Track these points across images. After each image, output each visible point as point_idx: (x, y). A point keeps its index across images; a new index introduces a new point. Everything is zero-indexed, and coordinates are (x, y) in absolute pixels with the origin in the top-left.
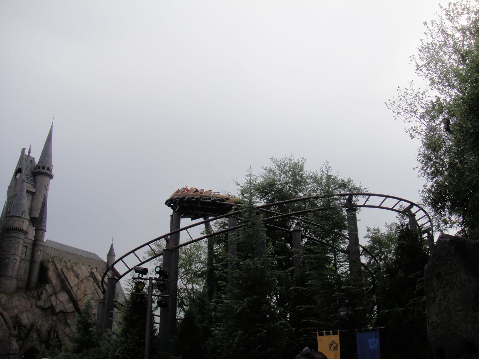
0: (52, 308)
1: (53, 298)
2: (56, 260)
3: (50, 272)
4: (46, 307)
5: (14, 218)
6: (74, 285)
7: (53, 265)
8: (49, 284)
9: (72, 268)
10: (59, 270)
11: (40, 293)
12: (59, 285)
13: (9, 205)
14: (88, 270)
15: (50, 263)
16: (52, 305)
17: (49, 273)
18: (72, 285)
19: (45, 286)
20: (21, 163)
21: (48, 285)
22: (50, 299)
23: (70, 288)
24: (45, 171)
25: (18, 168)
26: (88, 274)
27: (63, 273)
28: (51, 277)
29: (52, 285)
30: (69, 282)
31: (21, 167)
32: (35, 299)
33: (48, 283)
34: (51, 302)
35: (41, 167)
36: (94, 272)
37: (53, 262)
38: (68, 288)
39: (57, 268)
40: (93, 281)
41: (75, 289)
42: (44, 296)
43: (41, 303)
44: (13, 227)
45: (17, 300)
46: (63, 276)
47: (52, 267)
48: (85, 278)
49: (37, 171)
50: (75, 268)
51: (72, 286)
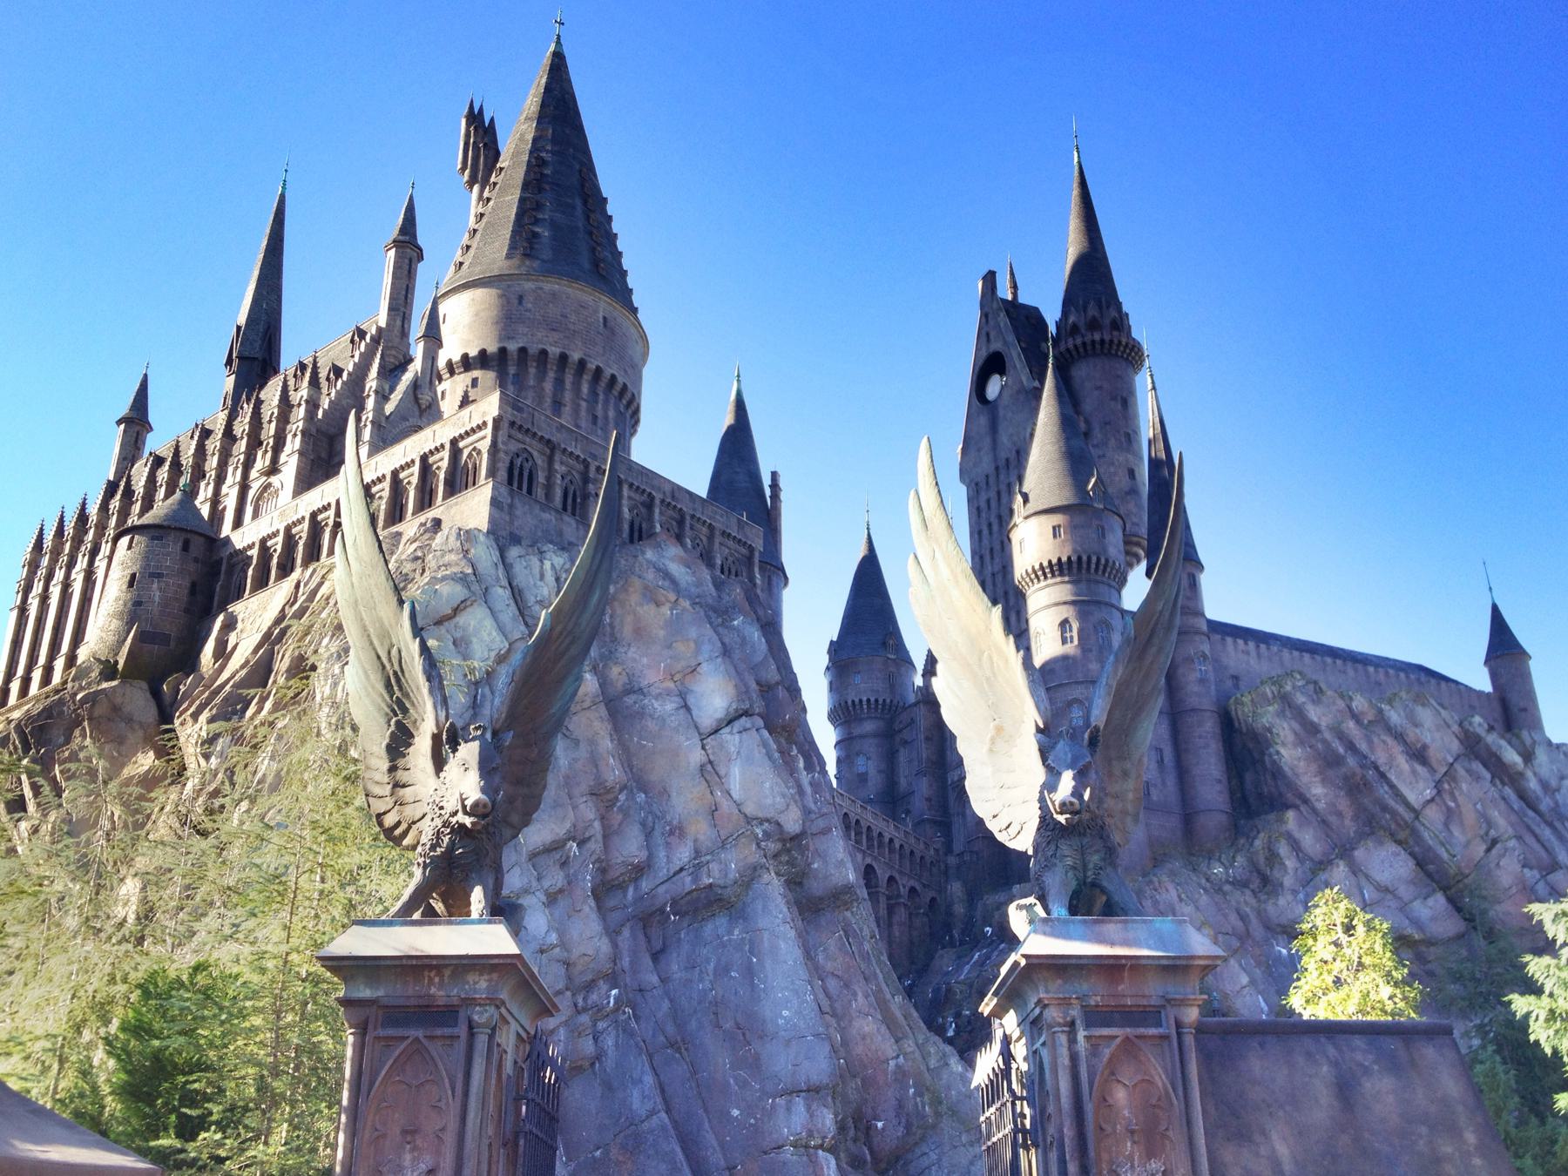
2: (1294, 687)
3: (1283, 751)
6: (1422, 800)
7: (1288, 713)
8: (1296, 807)
9: (1381, 720)
10: (1328, 735)
11: (1262, 860)
12: (1344, 804)
14: (1449, 726)
15: (1270, 708)
17: (1278, 753)
19: (1281, 821)
26: (1455, 746)
27: (1351, 747)
28: (1297, 775)
29: (1314, 811)
30: (1392, 786)
32: (1248, 892)
33: (1287, 807)
36: (1482, 732)
38: (1394, 813)
39: (1312, 729)
40: (1488, 776)
41: (1433, 815)
45: (1181, 900)
47: (1285, 725)
48: (1456, 760)
50: (1395, 717)
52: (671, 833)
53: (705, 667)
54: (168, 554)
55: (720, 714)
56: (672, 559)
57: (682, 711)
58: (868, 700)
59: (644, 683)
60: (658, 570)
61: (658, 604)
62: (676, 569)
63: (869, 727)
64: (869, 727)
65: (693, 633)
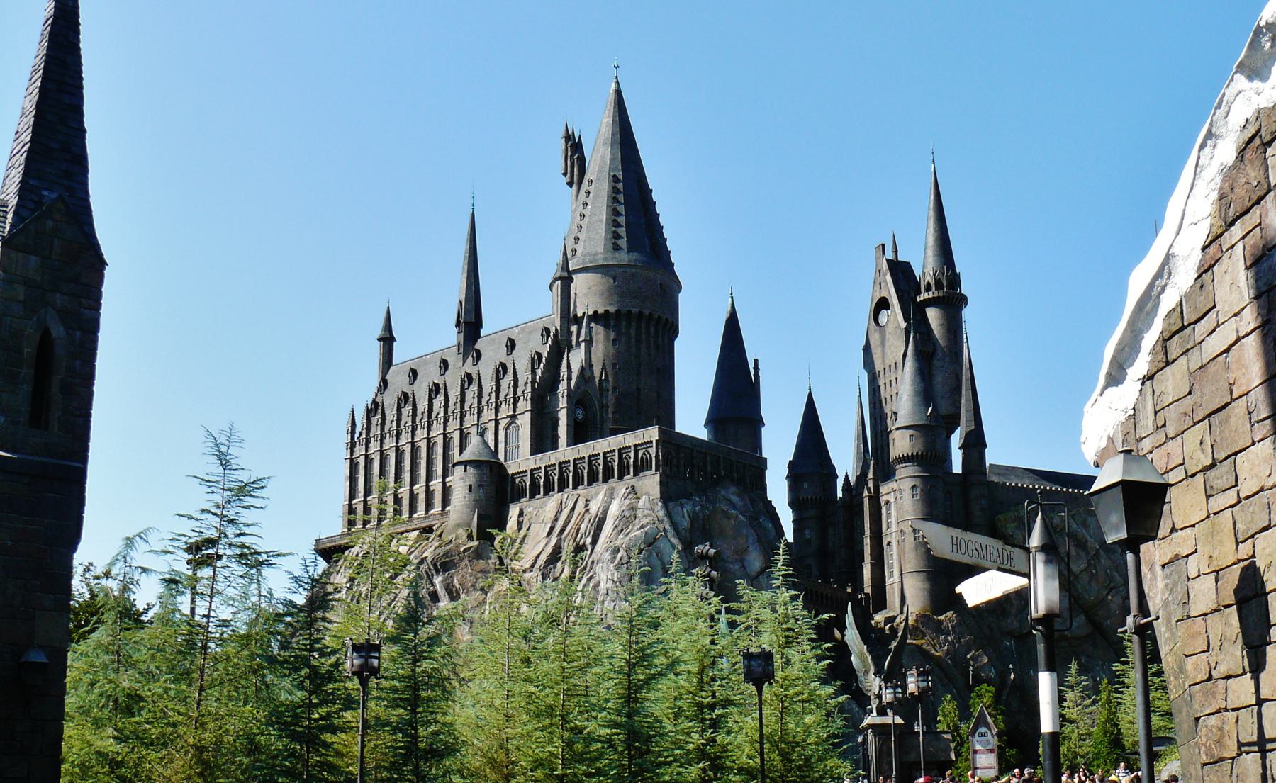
4: (1024, 632)
31: (884, 294)
53: (751, 548)
56: (733, 494)
58: (811, 498)
60: (727, 500)
62: (735, 498)
63: (812, 513)
64: (812, 513)
65: (745, 531)
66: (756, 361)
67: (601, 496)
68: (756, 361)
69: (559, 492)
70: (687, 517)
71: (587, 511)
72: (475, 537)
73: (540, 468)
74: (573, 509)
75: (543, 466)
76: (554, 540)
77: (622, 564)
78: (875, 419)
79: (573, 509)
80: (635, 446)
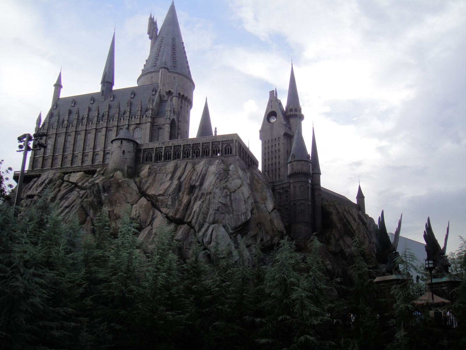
0: (342, 252)
1: (341, 242)
3: (334, 217)
4: (337, 252)
5: (302, 163)
8: (335, 228)
9: (349, 212)
10: (341, 214)
13: (267, 149)
16: (342, 250)
18: (355, 229)
20: (273, 107)
21: (334, 230)
22: (339, 244)
23: (353, 232)
24: (297, 113)
25: (270, 111)
27: (345, 217)
30: (351, 226)
34: (341, 246)
35: (293, 109)
37: (335, 206)
39: (339, 213)
42: (333, 241)
43: (332, 248)
44: (303, 172)
46: (345, 220)
49: (289, 114)
51: (355, 230)
52: (266, 233)
53: (268, 198)
54: (131, 147)
55: (272, 209)
57: (265, 208)
59: (258, 201)
61: (259, 183)
66: (216, 128)
67: (202, 163)
68: (216, 128)
69: (173, 160)
70: (249, 179)
71: (194, 170)
72: (126, 176)
73: (162, 147)
74: (185, 168)
75: (164, 147)
76: (176, 182)
77: (228, 196)
78: (265, 160)
79: (185, 168)
80: (222, 141)
